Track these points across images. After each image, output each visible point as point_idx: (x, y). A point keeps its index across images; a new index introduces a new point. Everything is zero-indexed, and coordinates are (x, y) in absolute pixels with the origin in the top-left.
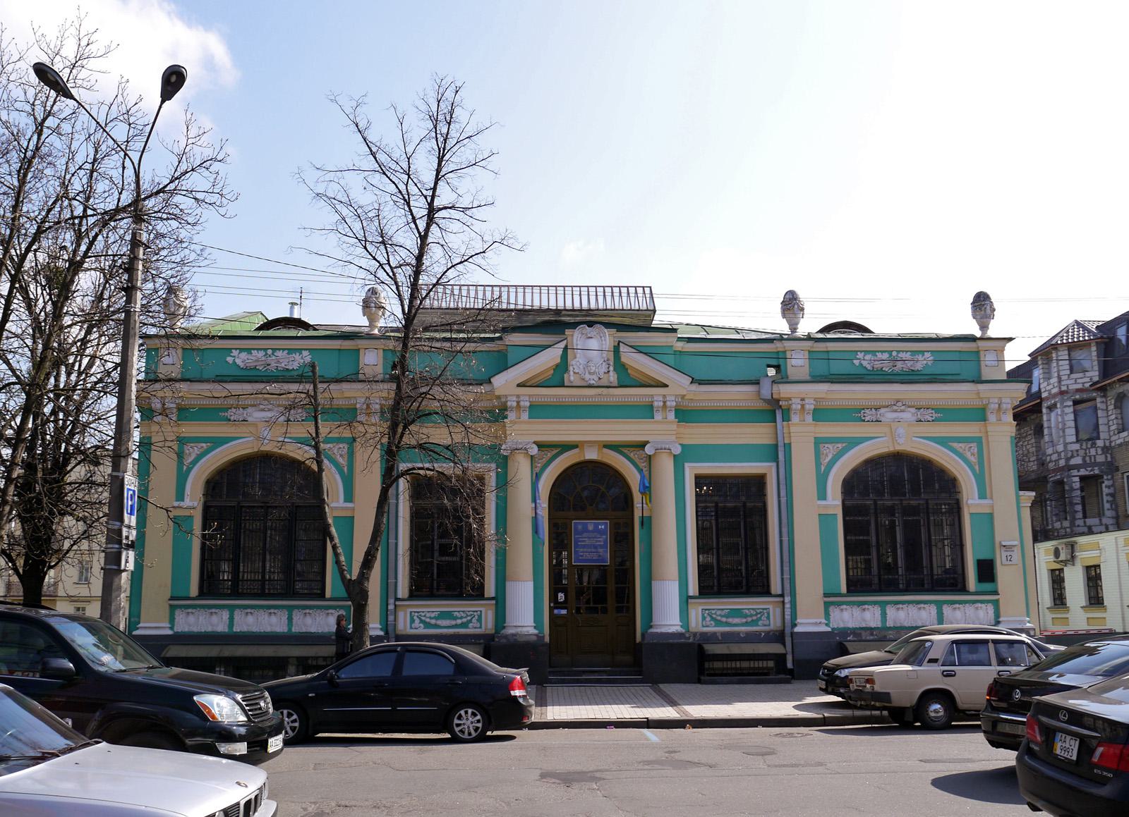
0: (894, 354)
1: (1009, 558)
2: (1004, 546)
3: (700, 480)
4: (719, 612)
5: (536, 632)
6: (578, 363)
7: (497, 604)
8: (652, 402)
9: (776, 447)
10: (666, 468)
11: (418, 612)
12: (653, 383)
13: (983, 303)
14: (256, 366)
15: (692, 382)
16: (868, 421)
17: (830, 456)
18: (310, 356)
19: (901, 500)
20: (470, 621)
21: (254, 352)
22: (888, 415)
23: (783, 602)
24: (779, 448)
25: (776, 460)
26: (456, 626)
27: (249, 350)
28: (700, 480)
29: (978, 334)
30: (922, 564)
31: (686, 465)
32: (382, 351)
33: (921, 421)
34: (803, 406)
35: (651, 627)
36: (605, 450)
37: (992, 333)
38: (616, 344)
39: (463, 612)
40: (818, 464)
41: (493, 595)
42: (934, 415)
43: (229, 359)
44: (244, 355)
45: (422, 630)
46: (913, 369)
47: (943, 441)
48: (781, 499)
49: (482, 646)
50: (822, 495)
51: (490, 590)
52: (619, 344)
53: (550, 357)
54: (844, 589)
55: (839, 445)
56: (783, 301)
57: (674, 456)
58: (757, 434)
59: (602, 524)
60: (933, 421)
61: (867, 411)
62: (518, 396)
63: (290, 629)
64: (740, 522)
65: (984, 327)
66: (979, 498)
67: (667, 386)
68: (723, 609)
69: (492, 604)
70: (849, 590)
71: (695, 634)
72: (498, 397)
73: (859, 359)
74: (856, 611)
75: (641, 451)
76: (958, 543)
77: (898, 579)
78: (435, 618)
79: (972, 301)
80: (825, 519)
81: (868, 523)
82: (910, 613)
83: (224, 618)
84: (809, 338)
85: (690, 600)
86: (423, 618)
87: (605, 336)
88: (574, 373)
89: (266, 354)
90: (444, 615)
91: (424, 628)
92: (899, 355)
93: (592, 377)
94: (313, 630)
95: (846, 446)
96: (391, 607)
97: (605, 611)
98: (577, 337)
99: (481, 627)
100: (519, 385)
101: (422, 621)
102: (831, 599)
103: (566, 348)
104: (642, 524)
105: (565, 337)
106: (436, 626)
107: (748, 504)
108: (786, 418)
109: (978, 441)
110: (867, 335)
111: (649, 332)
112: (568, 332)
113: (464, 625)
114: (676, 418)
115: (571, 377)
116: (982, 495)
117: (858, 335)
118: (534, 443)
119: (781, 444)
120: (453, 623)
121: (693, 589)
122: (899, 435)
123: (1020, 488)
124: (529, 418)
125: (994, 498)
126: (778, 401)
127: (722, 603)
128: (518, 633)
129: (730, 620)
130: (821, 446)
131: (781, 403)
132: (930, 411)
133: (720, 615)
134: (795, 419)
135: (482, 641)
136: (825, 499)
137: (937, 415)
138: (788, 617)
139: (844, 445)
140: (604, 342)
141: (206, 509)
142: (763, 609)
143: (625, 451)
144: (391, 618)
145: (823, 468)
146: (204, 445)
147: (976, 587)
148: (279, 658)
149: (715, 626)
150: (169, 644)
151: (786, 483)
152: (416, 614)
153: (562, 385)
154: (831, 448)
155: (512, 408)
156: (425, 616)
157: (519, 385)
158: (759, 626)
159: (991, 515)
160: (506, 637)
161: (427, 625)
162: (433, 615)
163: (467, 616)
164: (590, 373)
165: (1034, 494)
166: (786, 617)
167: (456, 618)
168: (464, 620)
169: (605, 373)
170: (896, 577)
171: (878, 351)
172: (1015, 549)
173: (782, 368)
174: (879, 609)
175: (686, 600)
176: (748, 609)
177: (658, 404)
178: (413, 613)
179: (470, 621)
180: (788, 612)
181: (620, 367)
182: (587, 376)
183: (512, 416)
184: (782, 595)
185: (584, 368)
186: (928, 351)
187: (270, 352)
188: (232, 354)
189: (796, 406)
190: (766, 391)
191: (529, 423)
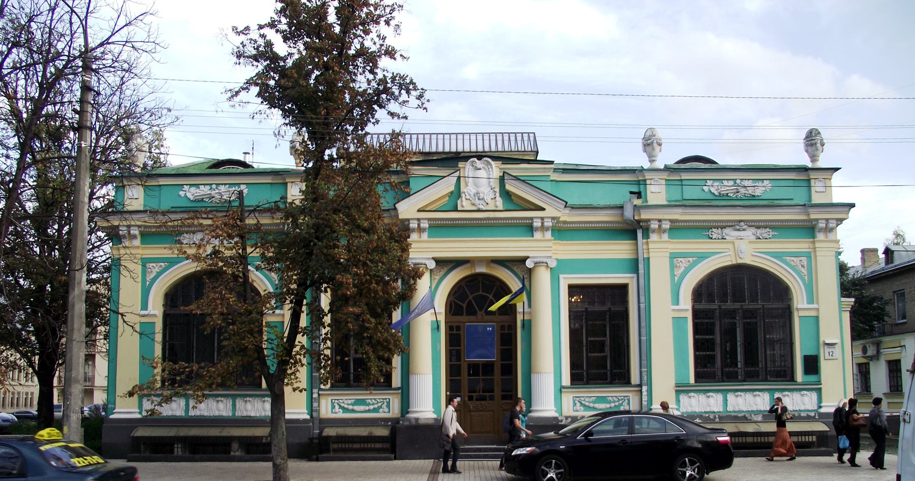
0: (738, 181)
1: (831, 354)
2: (827, 344)
3: (573, 289)
4: (587, 399)
5: (434, 416)
6: (469, 192)
7: (402, 393)
8: (532, 223)
9: (636, 261)
10: (543, 279)
11: (338, 400)
12: (533, 208)
13: (814, 138)
14: (203, 198)
15: (565, 207)
17: (682, 269)
18: (247, 189)
19: (742, 305)
20: (381, 407)
21: (202, 187)
22: (730, 233)
23: (641, 391)
24: (639, 262)
25: (636, 270)
26: (369, 411)
27: (197, 186)
28: (573, 289)
29: (810, 165)
30: (758, 359)
34: (660, 226)
36: (493, 265)
37: (821, 164)
38: (502, 174)
39: (375, 399)
40: (673, 275)
41: (399, 385)
42: (771, 233)
43: (182, 193)
44: (193, 189)
45: (341, 415)
46: (753, 194)
48: (641, 305)
49: (390, 427)
50: (676, 301)
51: (396, 381)
52: (504, 174)
53: (447, 185)
54: (692, 380)
55: (691, 259)
56: (644, 138)
57: (551, 268)
58: (620, 249)
59: (489, 326)
60: (770, 238)
61: (714, 230)
62: (419, 220)
63: (234, 414)
64: (605, 326)
65: (814, 158)
66: (808, 303)
68: (591, 397)
69: (398, 394)
70: (696, 382)
71: (567, 418)
72: (403, 221)
74: (702, 397)
75: (523, 265)
76: (788, 341)
77: (737, 372)
78: (353, 404)
79: (804, 137)
80: (678, 321)
81: (713, 324)
82: (747, 399)
83: (181, 404)
84: (667, 169)
85: (563, 390)
86: (342, 405)
87: (492, 168)
88: (466, 199)
89: (211, 188)
90: (358, 402)
91: (343, 413)
92: (742, 183)
93: (481, 202)
94: (253, 414)
95: (696, 260)
96: (315, 395)
97: (492, 398)
98: (467, 168)
99: (389, 412)
100: (419, 211)
101: (340, 407)
102: (681, 389)
103: (459, 177)
104: (523, 326)
105: (458, 169)
106: (353, 411)
107: (612, 309)
108: (646, 235)
109: (808, 256)
110: (714, 166)
111: (529, 163)
112: (461, 165)
113: (376, 410)
114: (552, 237)
115: (464, 204)
116: (811, 300)
117: (707, 166)
118: (433, 258)
119: (641, 259)
120: (367, 408)
121: (566, 380)
122: (741, 251)
123: (842, 293)
125: (820, 302)
126: (639, 222)
128: (420, 417)
130: (675, 260)
131: (641, 224)
132: (768, 230)
133: (589, 402)
134: (654, 237)
135: (390, 423)
136: (678, 305)
137: (773, 233)
138: (644, 403)
139: (694, 259)
140: (491, 172)
141: (166, 316)
142: (624, 396)
143: (510, 265)
144: (315, 405)
145: (676, 278)
146: (163, 264)
147: (802, 379)
148: (224, 437)
150: (137, 427)
151: (645, 291)
152: (336, 401)
153: (456, 210)
155: (413, 230)
156: (343, 403)
157: (419, 211)
159: (817, 318)
160: (409, 420)
161: (345, 410)
162: (350, 402)
163: (378, 402)
164: (479, 199)
165: (853, 300)
166: (643, 403)
167: (369, 404)
168: (376, 406)
169: (492, 199)
170: (736, 369)
172: (836, 346)
173: (643, 194)
175: (561, 389)
176: (611, 396)
177: (537, 224)
178: (333, 401)
179: (381, 407)
180: (645, 398)
181: (507, 195)
182: (477, 202)
183: (414, 237)
184: (640, 386)
185: (474, 195)
187: (214, 186)
188: (184, 189)
189: (654, 225)
190: (629, 213)
191: (429, 242)
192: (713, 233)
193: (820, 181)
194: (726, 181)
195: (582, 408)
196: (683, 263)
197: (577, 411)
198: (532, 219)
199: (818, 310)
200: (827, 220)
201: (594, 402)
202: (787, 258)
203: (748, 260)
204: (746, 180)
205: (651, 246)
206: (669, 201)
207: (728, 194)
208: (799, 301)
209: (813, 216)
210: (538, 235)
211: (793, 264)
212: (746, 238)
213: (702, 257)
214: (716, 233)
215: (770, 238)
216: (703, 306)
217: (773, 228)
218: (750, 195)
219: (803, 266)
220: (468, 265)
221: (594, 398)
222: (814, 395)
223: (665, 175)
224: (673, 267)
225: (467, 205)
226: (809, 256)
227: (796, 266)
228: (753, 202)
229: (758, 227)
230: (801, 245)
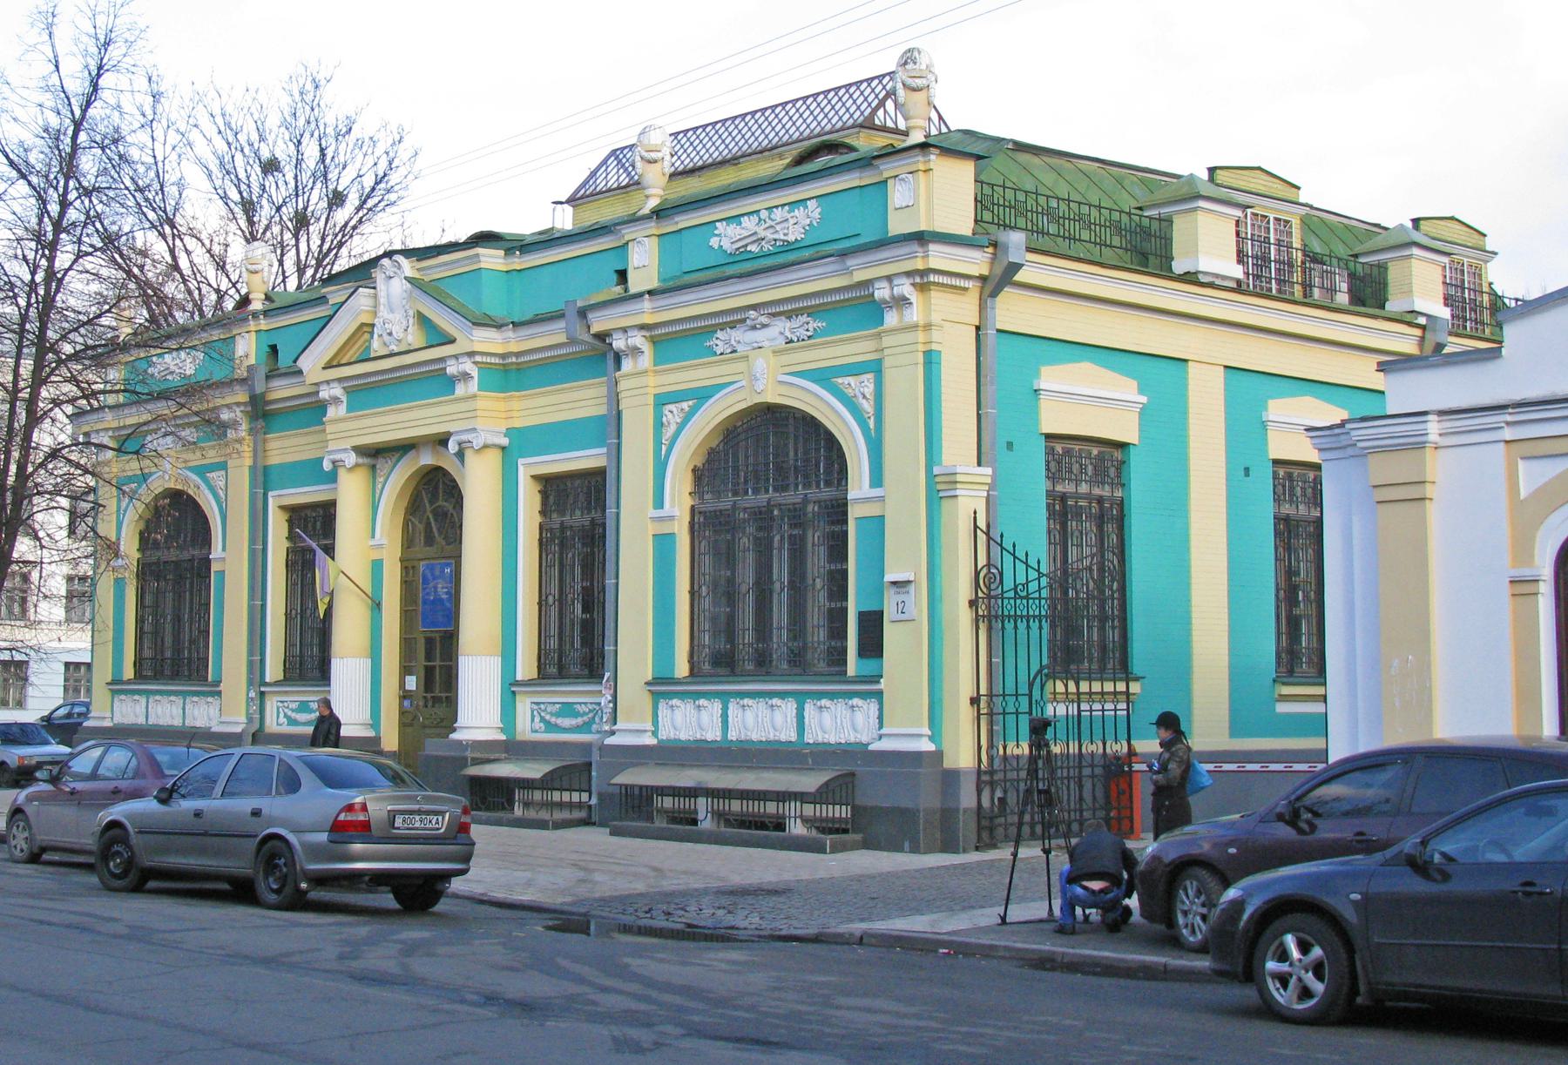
0: (764, 214)
1: (900, 606)
2: (894, 583)
8: (445, 368)
16: (722, 354)
17: (673, 428)
31: (521, 461)
32: (253, 334)
33: (791, 341)
35: (454, 730)
45: (287, 729)
46: (785, 238)
47: (823, 377)
54: (682, 669)
55: (685, 405)
61: (719, 334)
67: (452, 341)
68: (554, 703)
73: (719, 235)
80: (664, 542)
95: (695, 404)
100: (328, 366)
102: (662, 686)
116: (877, 479)
118: (357, 449)
121: (526, 667)
124: (348, 412)
127: (564, 692)
129: (559, 721)
132: (804, 318)
133: (551, 714)
139: (691, 403)
149: (545, 732)
154: (675, 412)
157: (328, 366)
158: (590, 732)
162: (294, 706)
171: (743, 215)
172: (912, 588)
174: (721, 706)
175: (511, 688)
176: (580, 703)
186: (813, 198)
192: (718, 342)
193: (903, 180)
194: (746, 218)
195: (542, 725)
196: (673, 414)
197: (536, 731)
198: (442, 360)
199: (882, 499)
200: (889, 278)
201: (558, 715)
202: (840, 380)
203: (771, 397)
204: (776, 207)
205: (623, 385)
206: (665, 280)
207: (746, 245)
208: (858, 486)
209: (860, 276)
210: (460, 390)
211: (850, 392)
212: (766, 344)
213: (702, 395)
214: (720, 341)
215: (809, 337)
216: (711, 503)
217: (811, 312)
218: (784, 241)
219: (864, 397)
220: (412, 453)
221: (558, 706)
222: (873, 707)
223: (652, 227)
224: (659, 425)
225: (377, 347)
226: (875, 368)
227: (855, 396)
228: (785, 259)
229: (789, 315)
230: (853, 349)
